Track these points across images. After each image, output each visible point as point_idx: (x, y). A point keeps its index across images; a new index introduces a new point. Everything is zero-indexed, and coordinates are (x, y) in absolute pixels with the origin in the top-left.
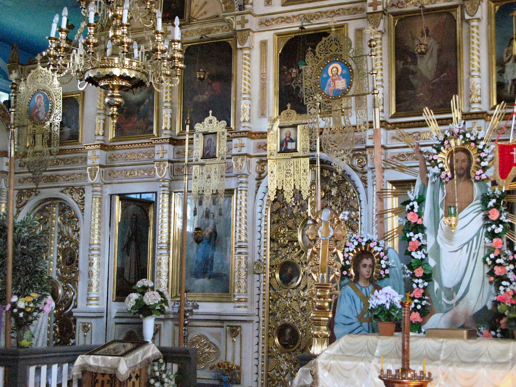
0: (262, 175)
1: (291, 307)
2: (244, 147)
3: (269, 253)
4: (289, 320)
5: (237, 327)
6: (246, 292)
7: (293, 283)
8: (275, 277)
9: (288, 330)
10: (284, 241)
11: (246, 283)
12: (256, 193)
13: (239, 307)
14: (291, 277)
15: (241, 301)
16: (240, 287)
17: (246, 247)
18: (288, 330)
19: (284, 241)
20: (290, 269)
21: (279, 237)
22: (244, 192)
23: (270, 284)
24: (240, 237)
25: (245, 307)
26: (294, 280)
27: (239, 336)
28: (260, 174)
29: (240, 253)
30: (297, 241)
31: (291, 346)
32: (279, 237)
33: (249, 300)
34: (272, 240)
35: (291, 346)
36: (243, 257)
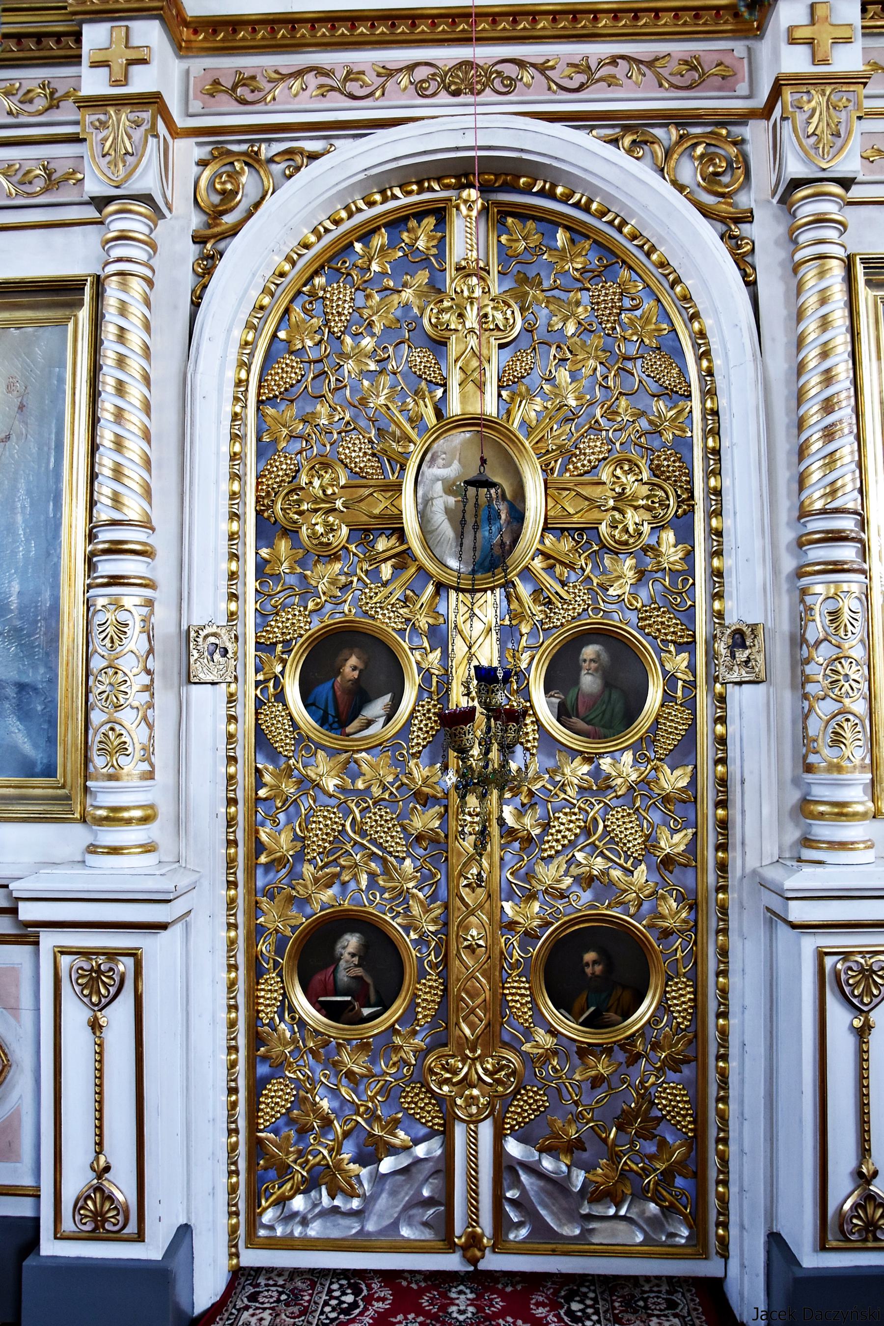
0: (229, 219)
1: (363, 834)
2: (144, 61)
3: (252, 584)
4: (359, 893)
5: (112, 955)
6: (149, 775)
7: (369, 723)
8: (280, 696)
9: (351, 942)
10: (331, 529)
11: (150, 726)
12: (196, 304)
13: (115, 851)
14: (360, 696)
15: (129, 821)
16: (122, 748)
17: (146, 553)
18: (351, 942)
19: (331, 529)
20: (353, 661)
21: (301, 513)
22: (136, 285)
23: (258, 726)
24: (116, 500)
25: (148, 848)
26: (377, 708)
27: (126, 1001)
28: (216, 214)
29: (115, 581)
30: (400, 534)
31: (366, 1011)
32: (301, 513)
33: (165, 810)
34: (268, 529)
35: (366, 1011)
36: (131, 598)
